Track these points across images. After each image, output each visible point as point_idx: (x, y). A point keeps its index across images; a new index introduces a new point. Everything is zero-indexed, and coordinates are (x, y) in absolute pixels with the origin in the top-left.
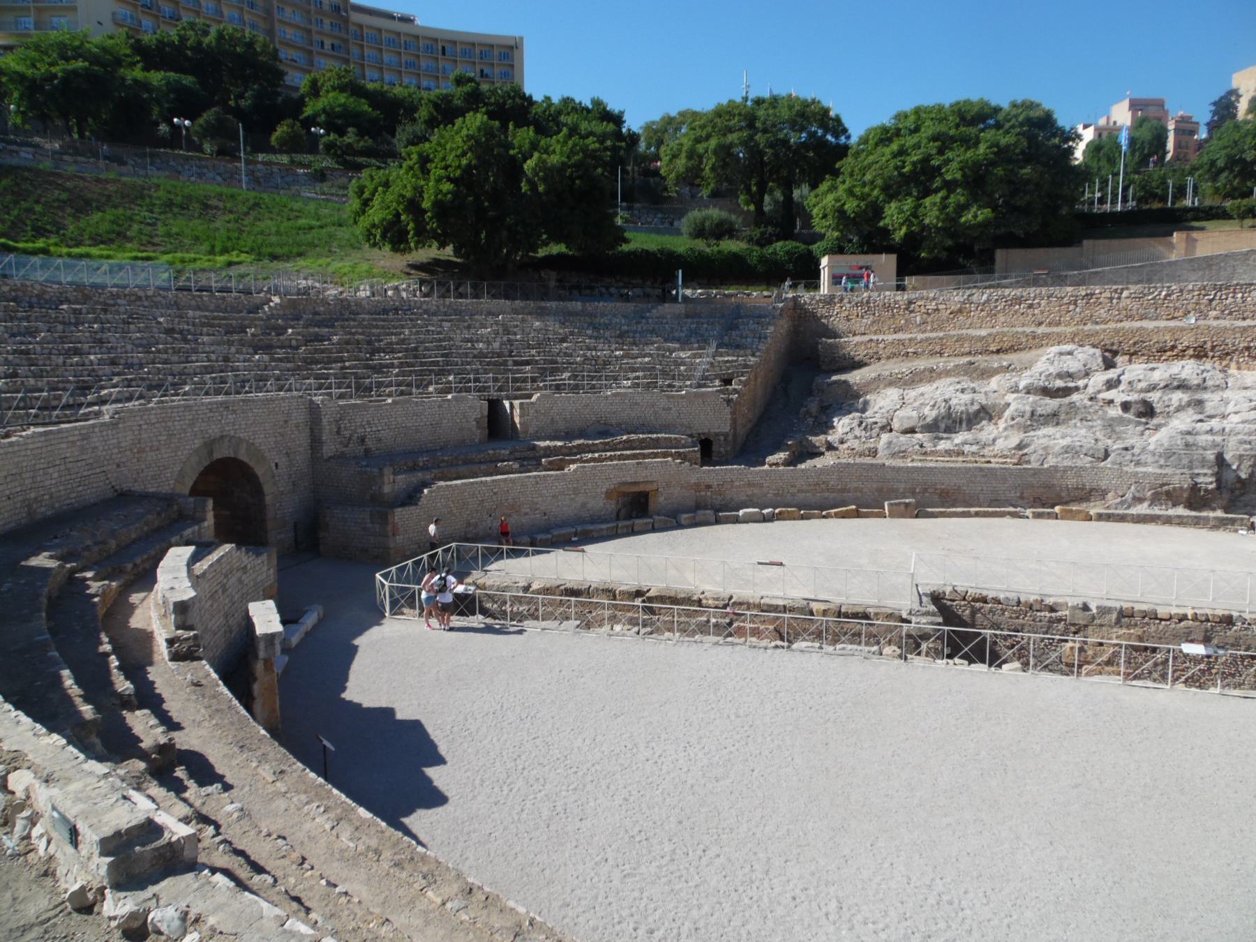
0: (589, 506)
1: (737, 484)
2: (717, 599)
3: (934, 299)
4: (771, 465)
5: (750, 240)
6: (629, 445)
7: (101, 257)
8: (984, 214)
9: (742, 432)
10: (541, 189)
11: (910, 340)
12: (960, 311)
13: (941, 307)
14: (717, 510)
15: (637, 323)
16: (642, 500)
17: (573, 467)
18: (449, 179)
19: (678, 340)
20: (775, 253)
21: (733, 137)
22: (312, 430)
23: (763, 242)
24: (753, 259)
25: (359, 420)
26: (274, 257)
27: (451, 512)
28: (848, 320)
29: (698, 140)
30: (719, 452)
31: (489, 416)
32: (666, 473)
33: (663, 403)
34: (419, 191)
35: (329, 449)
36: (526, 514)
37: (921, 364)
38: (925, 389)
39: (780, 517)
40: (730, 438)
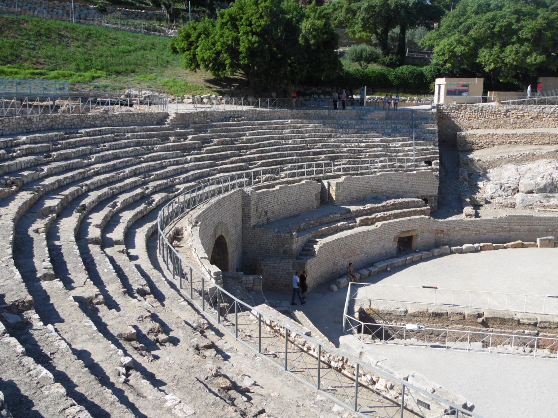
1: (457, 229)
2: (530, 319)
3: (522, 110)
5: (384, 64)
6: (395, 207)
7: (11, 73)
8: (541, 58)
10: (312, 42)
11: (513, 134)
12: (537, 117)
13: (525, 114)
14: (450, 246)
18: (253, 33)
19: (389, 135)
20: (402, 73)
22: (243, 210)
23: (392, 65)
24: (391, 77)
26: (118, 73)
28: (469, 120)
32: (419, 222)
34: (237, 40)
35: (253, 221)
36: (358, 254)
37: (526, 150)
38: (529, 165)
39: (482, 249)
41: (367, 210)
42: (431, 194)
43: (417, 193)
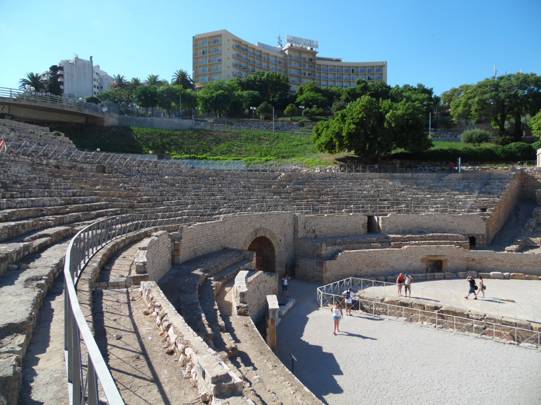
0: (413, 265)
1: (489, 259)
2: (478, 315)
4: (508, 251)
5: (497, 143)
6: (433, 238)
7: (223, 159)
9: (492, 234)
10: (393, 125)
15: (438, 182)
16: (439, 264)
17: (405, 247)
18: (354, 123)
19: (458, 190)
20: (510, 148)
21: (487, 96)
22: (294, 226)
23: (504, 143)
25: (313, 223)
26: (283, 157)
27: (350, 264)
29: (469, 98)
30: (479, 244)
31: (368, 223)
32: (452, 252)
33: (450, 219)
34: (341, 129)
35: (301, 234)
39: (514, 277)
40: (486, 237)
41: (405, 238)
42: (478, 233)
43: (464, 231)
